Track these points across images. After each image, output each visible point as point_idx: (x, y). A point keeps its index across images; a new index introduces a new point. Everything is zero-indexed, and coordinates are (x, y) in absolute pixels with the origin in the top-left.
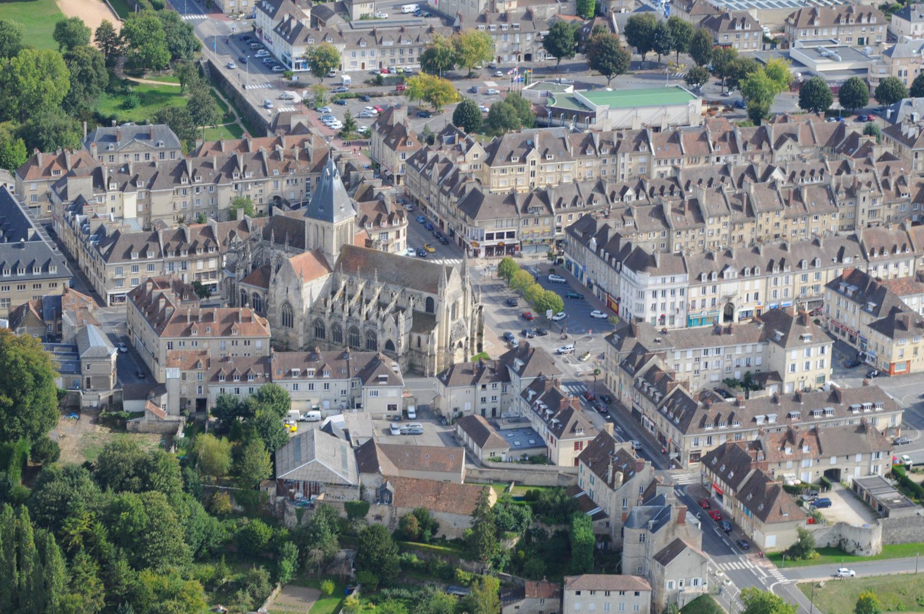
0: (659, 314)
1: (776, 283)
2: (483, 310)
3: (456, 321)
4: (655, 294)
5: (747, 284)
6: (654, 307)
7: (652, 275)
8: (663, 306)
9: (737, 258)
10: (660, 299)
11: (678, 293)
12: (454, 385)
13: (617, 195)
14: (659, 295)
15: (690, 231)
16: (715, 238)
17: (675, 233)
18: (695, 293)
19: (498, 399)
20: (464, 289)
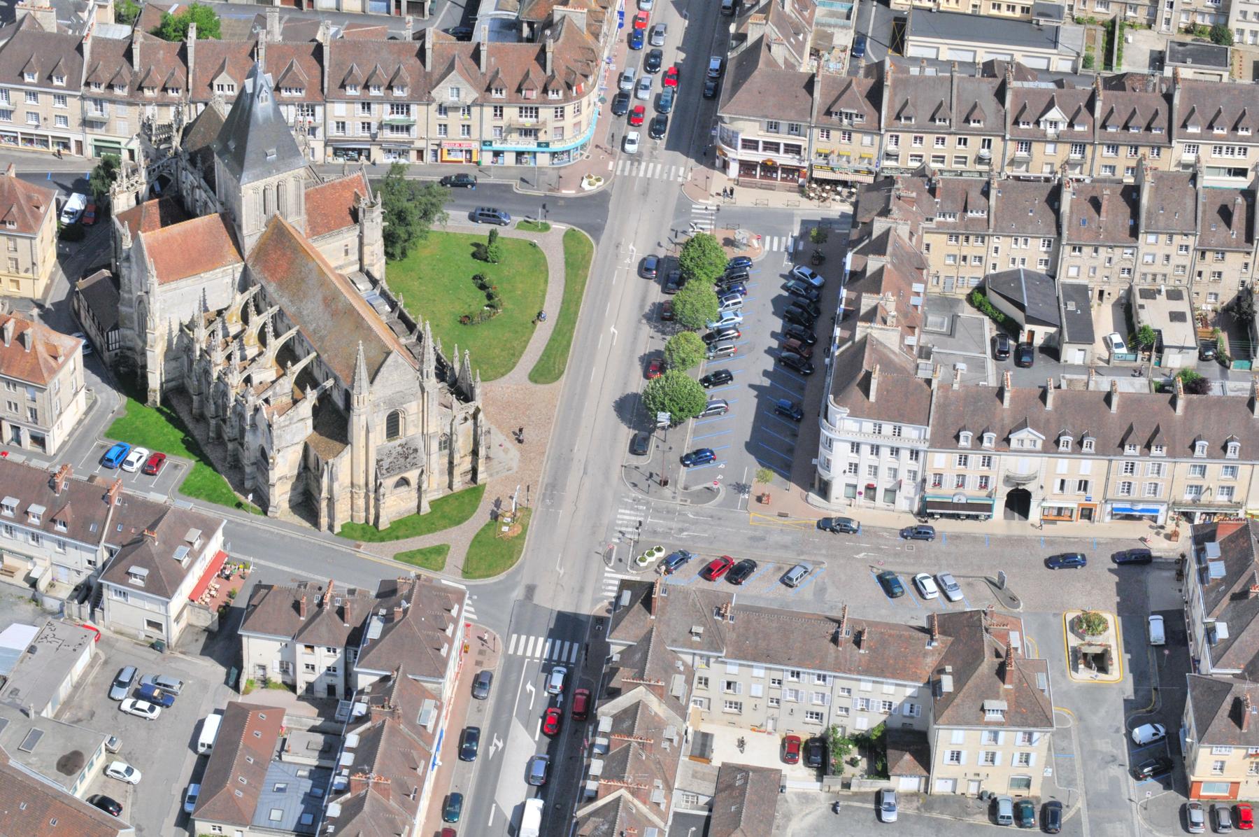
0: (863, 480)
1: (1131, 468)
2: (481, 416)
3: (398, 442)
4: (856, 447)
5: (1063, 466)
6: (854, 468)
7: (853, 414)
8: (875, 470)
9: (1056, 408)
10: (866, 457)
11: (905, 454)
12: (254, 630)
13: (1030, 114)
14: (866, 450)
15: (1101, 250)
16: (1158, 268)
17: (1068, 249)
18: (942, 461)
19: (341, 672)
20: (423, 389)
